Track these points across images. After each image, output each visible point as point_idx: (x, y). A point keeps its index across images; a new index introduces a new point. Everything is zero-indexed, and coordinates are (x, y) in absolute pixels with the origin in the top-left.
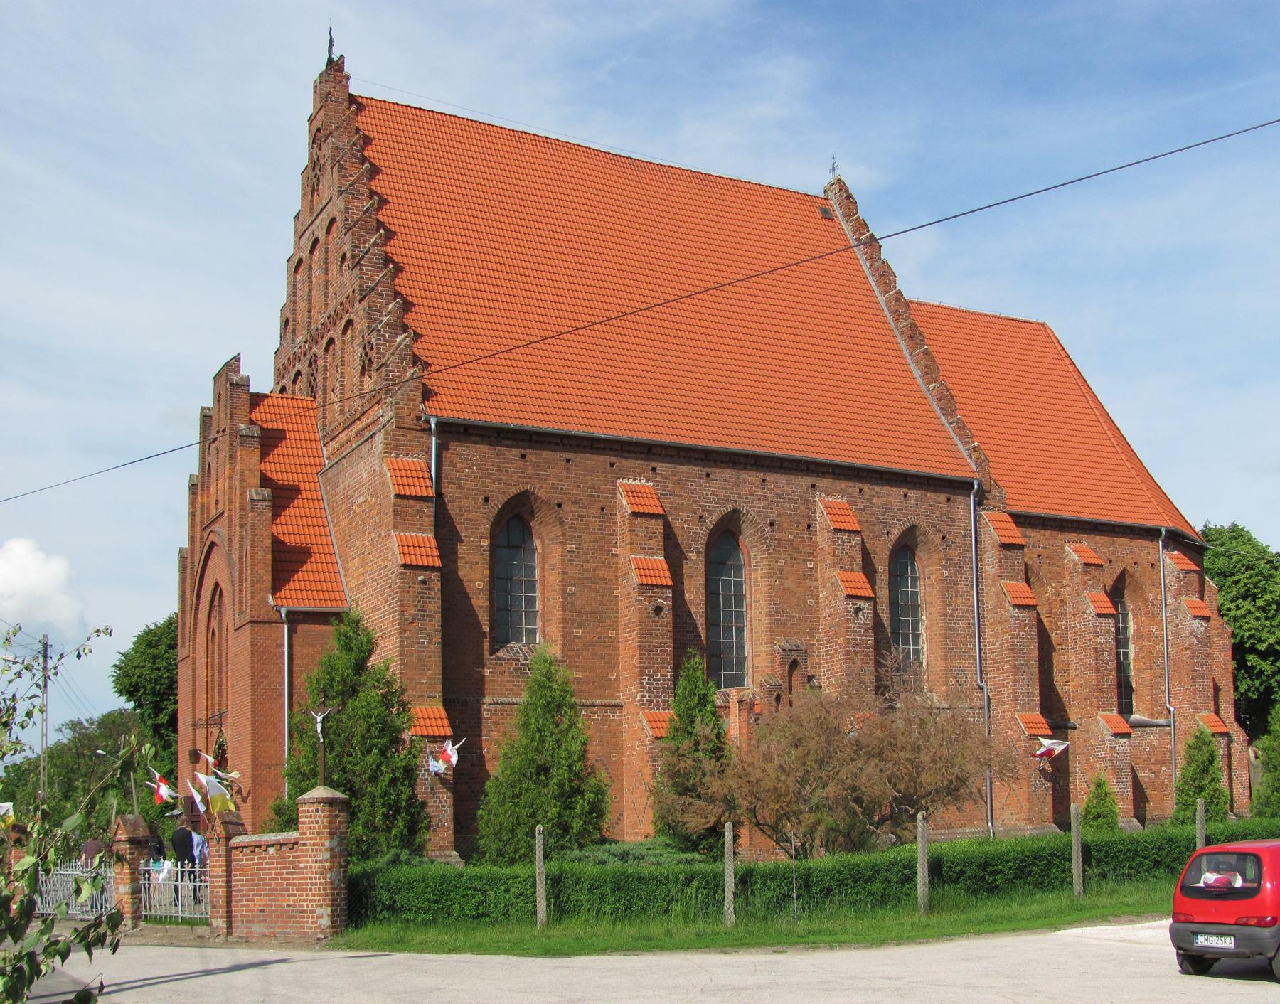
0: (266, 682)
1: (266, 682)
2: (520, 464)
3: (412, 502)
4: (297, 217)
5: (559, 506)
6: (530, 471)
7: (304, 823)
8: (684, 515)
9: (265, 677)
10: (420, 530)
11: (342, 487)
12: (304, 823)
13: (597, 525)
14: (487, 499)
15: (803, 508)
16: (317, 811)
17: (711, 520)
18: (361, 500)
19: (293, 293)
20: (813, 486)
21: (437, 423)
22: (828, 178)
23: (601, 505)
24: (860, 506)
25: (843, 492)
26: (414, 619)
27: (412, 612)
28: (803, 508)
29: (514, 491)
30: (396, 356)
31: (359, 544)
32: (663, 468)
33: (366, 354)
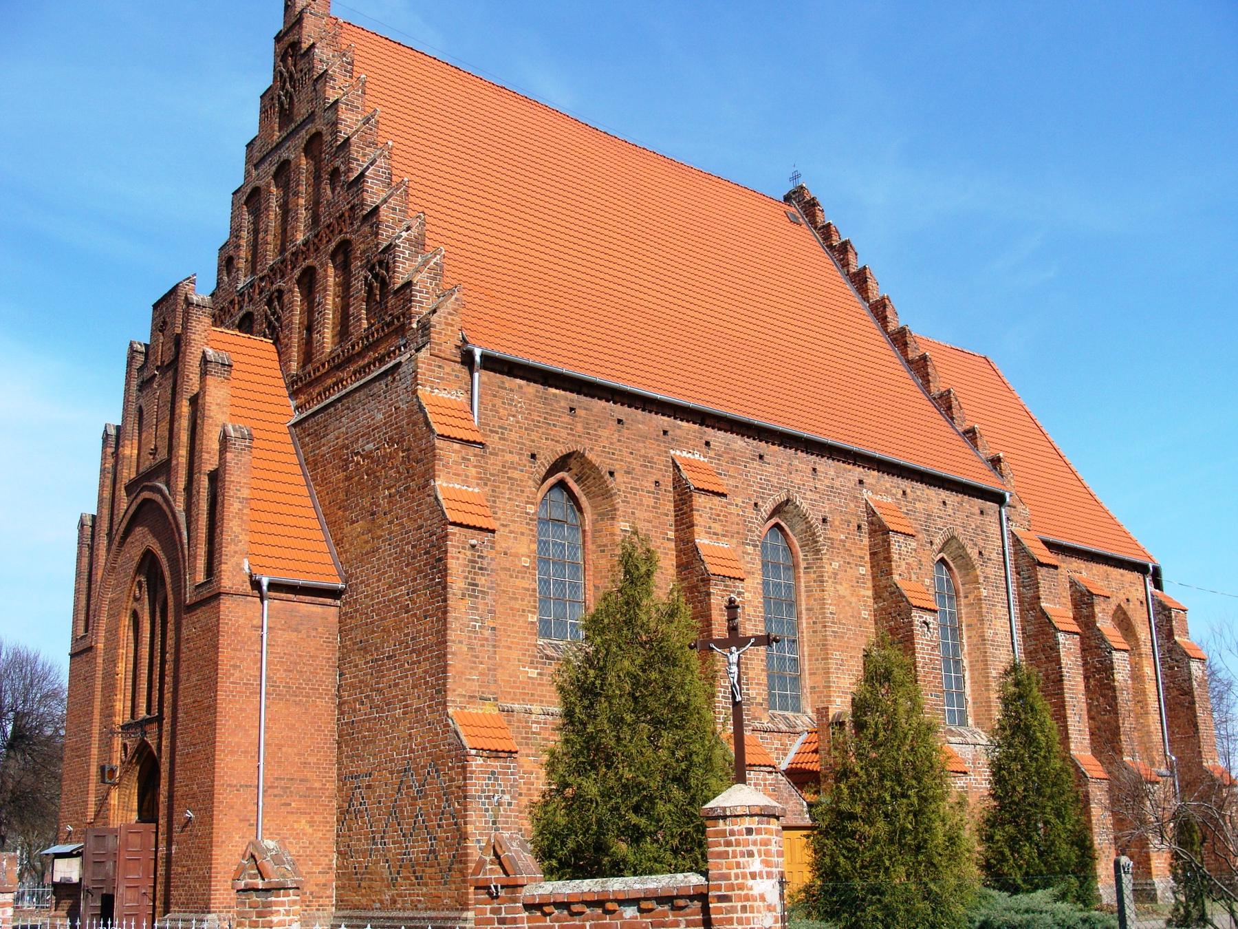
0: (237, 674)
1: (237, 674)
2: (567, 419)
3: (456, 446)
4: (250, 146)
5: (611, 474)
6: (579, 427)
7: (724, 855)
8: (739, 501)
9: (235, 667)
10: (465, 482)
11: (331, 436)
12: (724, 855)
13: (652, 502)
14: (533, 456)
15: (852, 505)
16: (749, 831)
17: (767, 507)
18: (370, 446)
19: (235, 232)
20: (861, 482)
21: (482, 356)
22: (789, 187)
23: (655, 478)
24: (904, 510)
25: (887, 492)
26: (464, 595)
27: (462, 585)
28: (852, 505)
29: (562, 450)
30: (424, 274)
31: (366, 502)
32: (719, 438)
33: (376, 276)
